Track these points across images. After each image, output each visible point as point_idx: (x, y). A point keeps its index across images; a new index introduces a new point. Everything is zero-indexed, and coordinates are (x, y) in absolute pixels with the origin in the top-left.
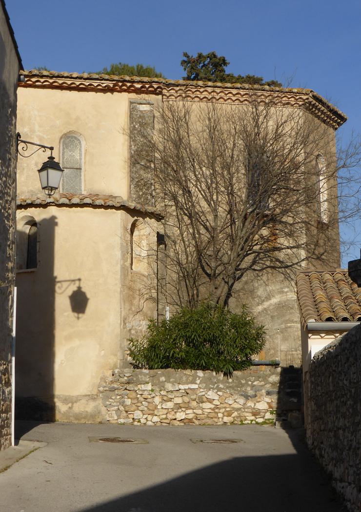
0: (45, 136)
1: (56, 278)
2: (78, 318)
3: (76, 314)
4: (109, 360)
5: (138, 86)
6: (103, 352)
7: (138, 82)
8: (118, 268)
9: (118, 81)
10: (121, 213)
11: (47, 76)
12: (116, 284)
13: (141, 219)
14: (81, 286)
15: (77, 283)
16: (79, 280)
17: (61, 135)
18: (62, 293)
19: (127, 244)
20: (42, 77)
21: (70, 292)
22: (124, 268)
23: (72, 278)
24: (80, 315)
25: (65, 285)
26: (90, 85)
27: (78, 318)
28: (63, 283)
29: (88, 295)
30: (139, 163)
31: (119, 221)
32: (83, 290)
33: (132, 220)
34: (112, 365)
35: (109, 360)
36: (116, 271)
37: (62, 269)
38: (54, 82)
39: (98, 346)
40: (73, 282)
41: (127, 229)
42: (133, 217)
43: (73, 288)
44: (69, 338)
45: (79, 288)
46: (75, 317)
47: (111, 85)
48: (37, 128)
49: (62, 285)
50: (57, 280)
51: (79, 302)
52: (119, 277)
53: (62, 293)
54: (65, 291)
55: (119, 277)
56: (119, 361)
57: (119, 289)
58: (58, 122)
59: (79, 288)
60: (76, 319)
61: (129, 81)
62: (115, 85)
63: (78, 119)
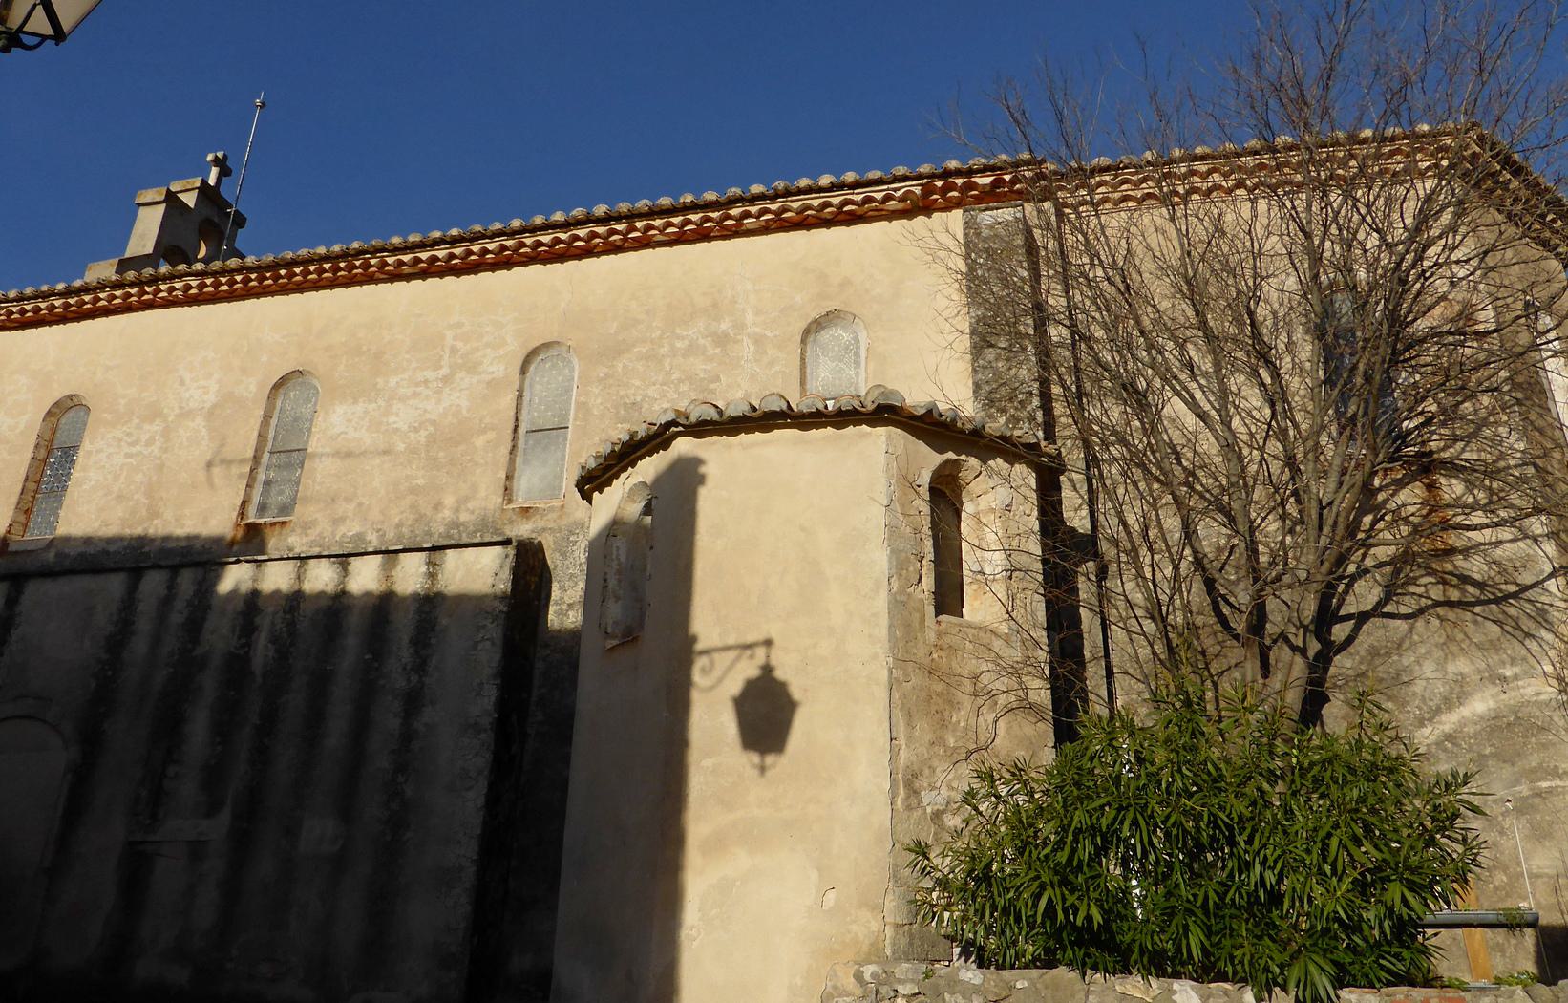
0: (768, 334)
1: (694, 639)
2: (763, 769)
3: (755, 758)
4: (854, 928)
5: (985, 180)
6: (831, 895)
7: (984, 170)
8: (881, 602)
9: (932, 176)
10: (882, 437)
11: (762, 197)
12: (875, 657)
13: (973, 461)
14: (773, 662)
15: (761, 653)
16: (768, 643)
17: (803, 325)
18: (711, 688)
19: (917, 531)
20: (753, 199)
21: (734, 686)
22: (904, 604)
23: (750, 638)
24: (770, 759)
25: (723, 660)
26: (869, 200)
27: (763, 769)
28: (716, 656)
29: (796, 693)
30: (992, 346)
31: (882, 459)
32: (780, 674)
33: (935, 459)
34: (865, 948)
35: (854, 928)
36: (874, 615)
37: (710, 620)
38: (785, 210)
39: (814, 875)
40: (748, 652)
41: (915, 487)
42: (941, 452)
43: (749, 669)
44: (718, 844)
45: (767, 669)
46: (754, 766)
47: (917, 190)
48: (749, 317)
49: (712, 663)
50: (699, 646)
51: (766, 714)
52: (885, 631)
53: (711, 688)
54: (720, 680)
55: (882, 631)
56: (889, 932)
57: (885, 673)
58: (798, 298)
59: (767, 669)
60: (755, 773)
61: (958, 173)
62: (928, 191)
63: (846, 283)
